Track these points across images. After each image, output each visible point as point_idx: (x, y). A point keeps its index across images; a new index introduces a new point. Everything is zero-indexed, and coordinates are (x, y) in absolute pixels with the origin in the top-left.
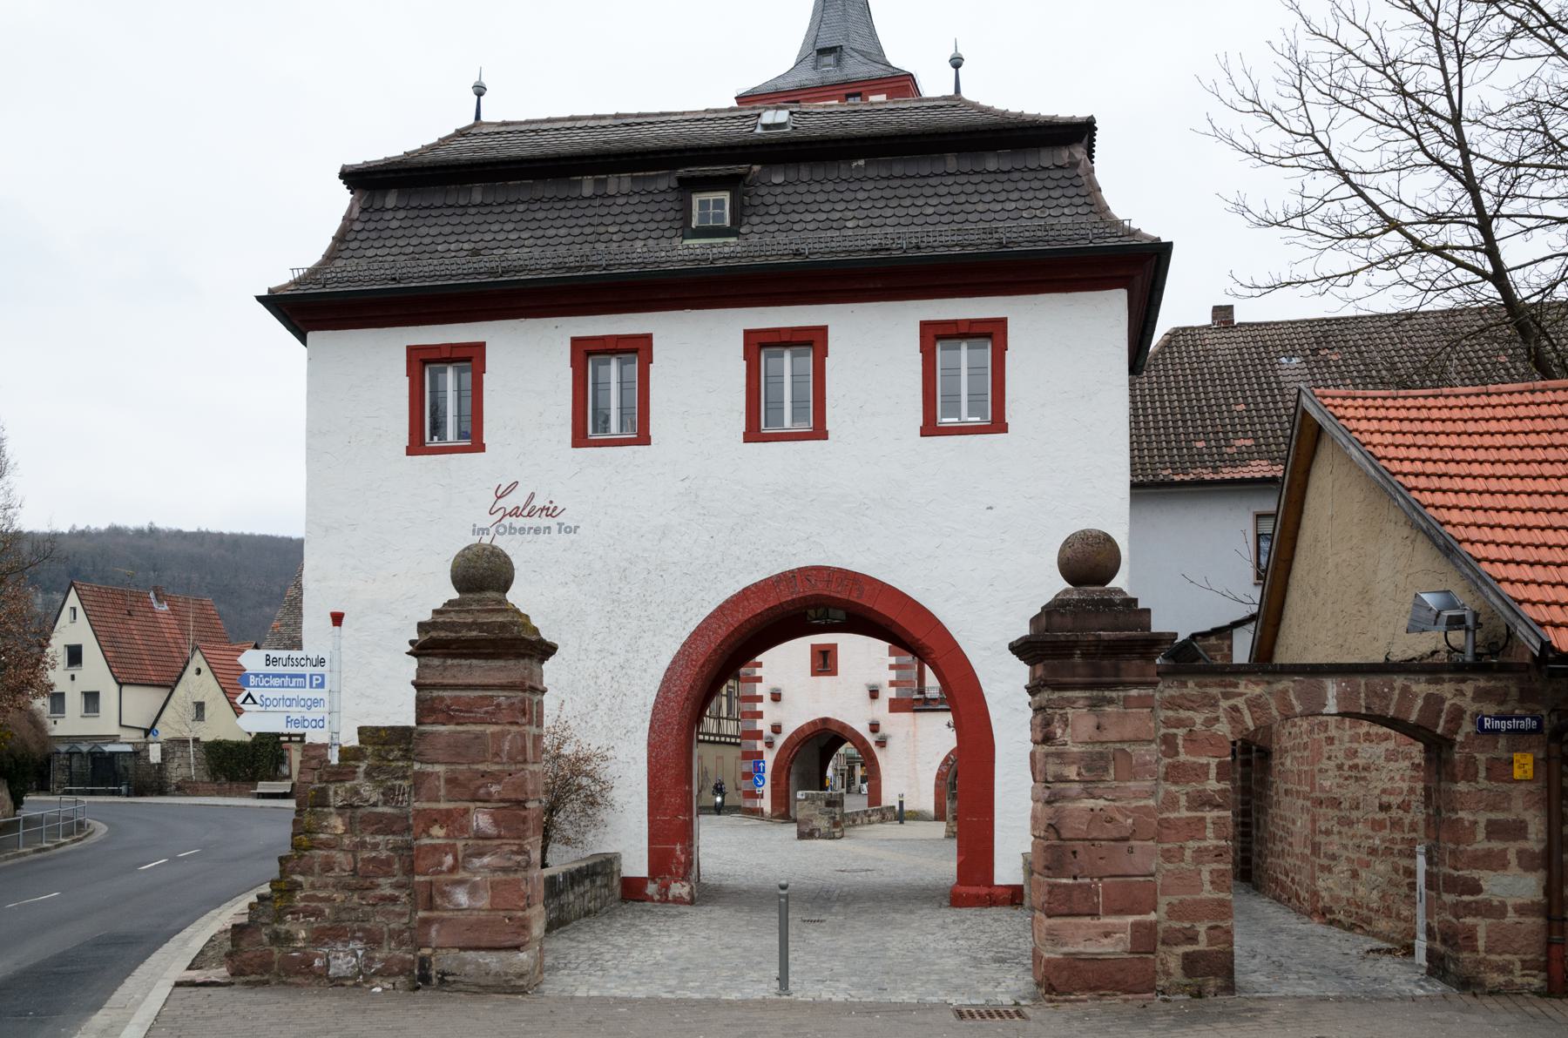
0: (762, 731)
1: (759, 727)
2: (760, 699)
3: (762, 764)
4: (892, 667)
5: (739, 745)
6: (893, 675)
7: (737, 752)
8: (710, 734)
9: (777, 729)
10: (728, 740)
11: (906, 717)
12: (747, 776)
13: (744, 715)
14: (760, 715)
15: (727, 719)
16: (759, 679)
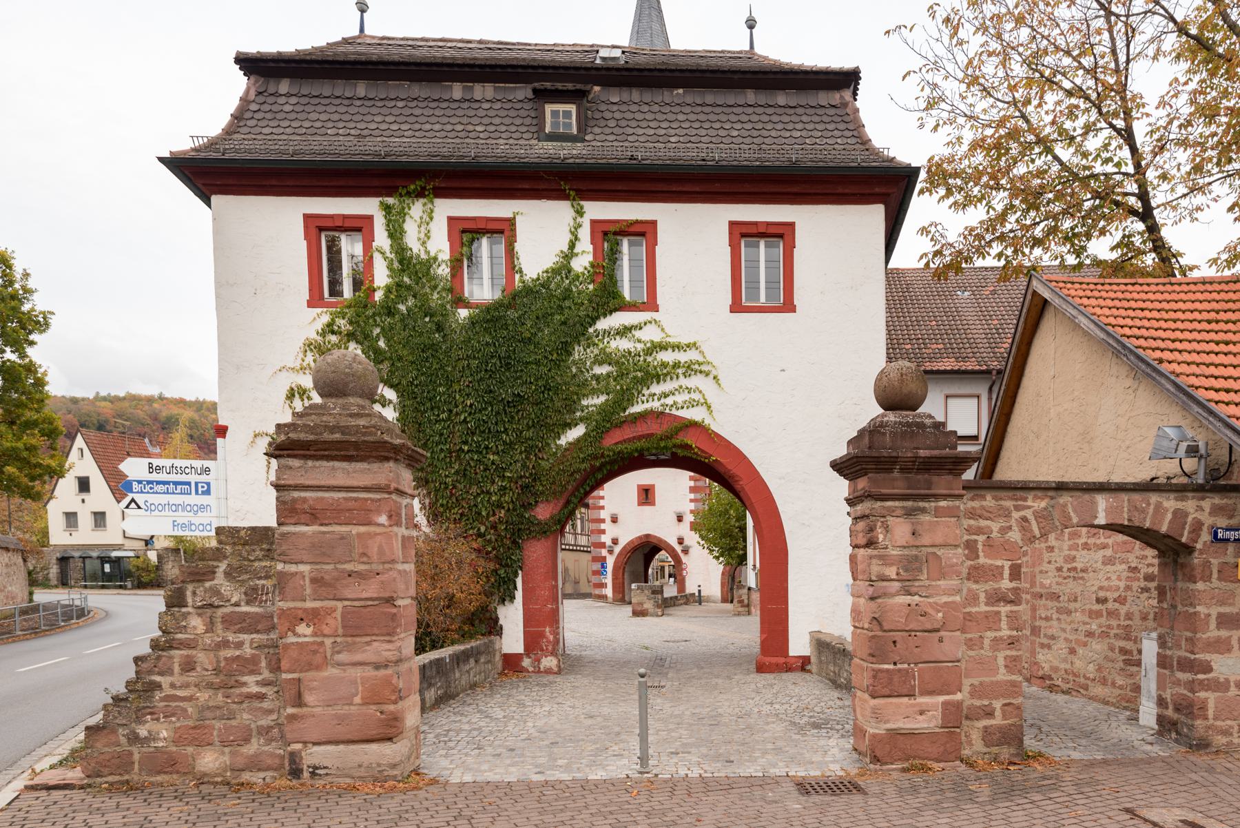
1: (603, 540)
2: (603, 521)
4: (691, 501)
6: (692, 506)
7: (588, 557)
8: (569, 545)
9: (615, 541)
12: (596, 573)
14: (603, 532)
16: (602, 508)
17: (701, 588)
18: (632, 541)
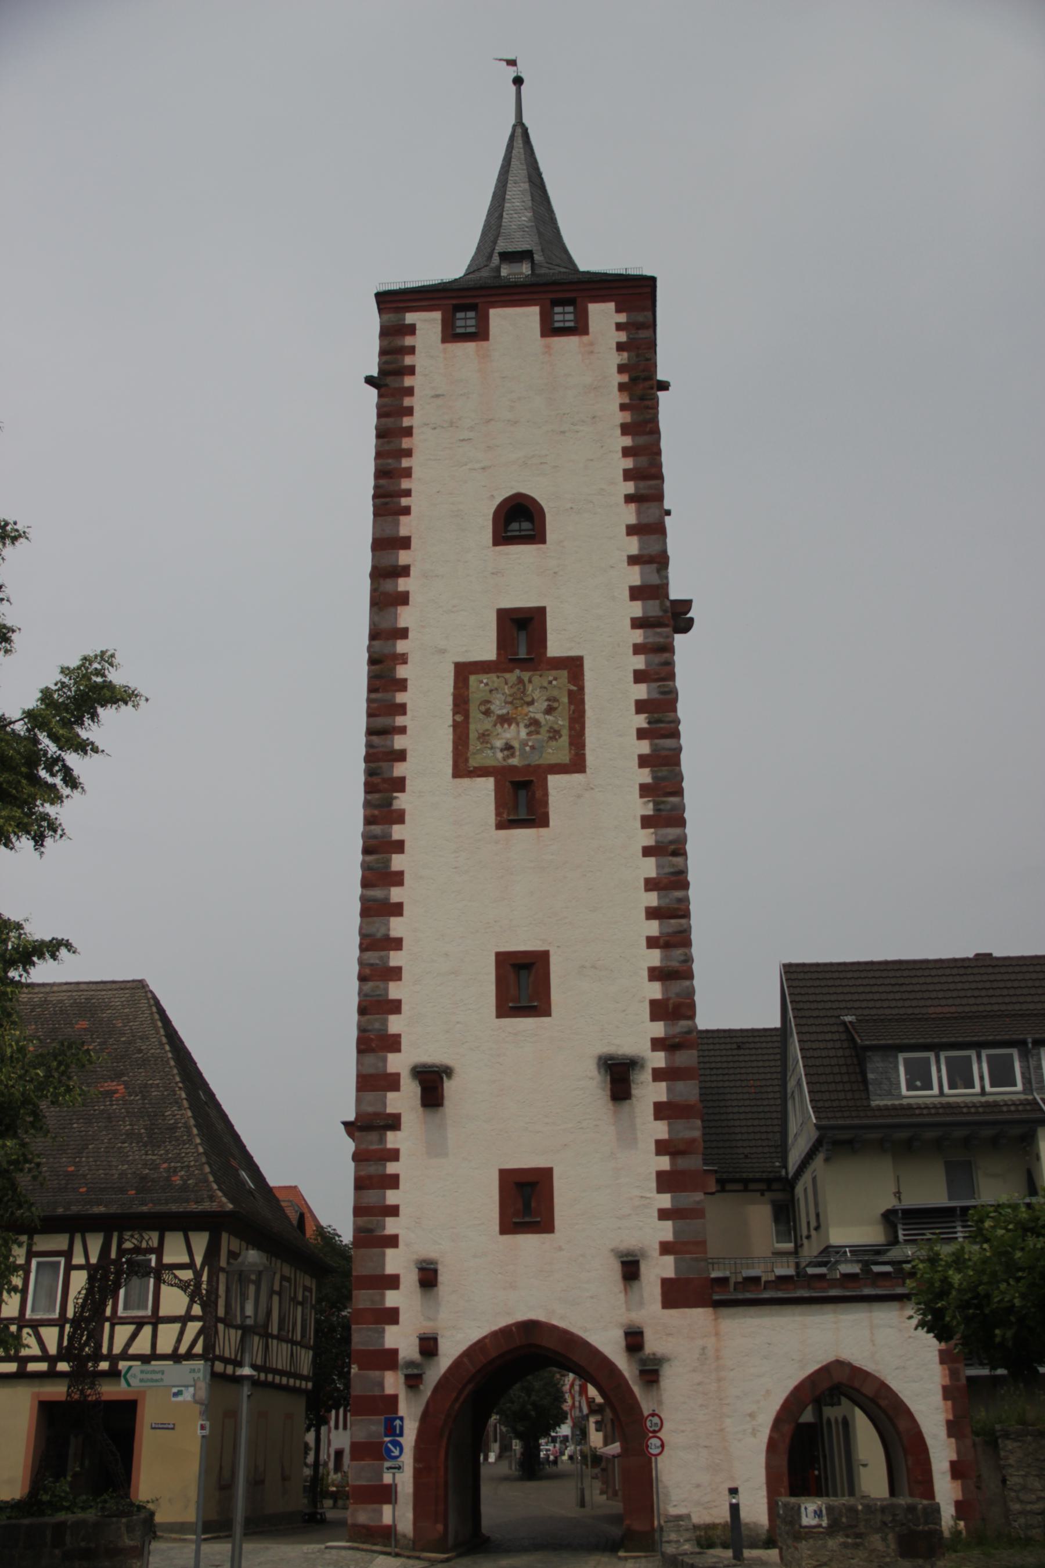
0: (395, 1352)
1: (390, 1342)
2: (393, 1282)
4: (664, 1214)
6: (666, 1231)
9: (429, 1346)
11: (700, 1316)
14: (392, 1316)
16: (393, 1241)
18: (477, 1348)
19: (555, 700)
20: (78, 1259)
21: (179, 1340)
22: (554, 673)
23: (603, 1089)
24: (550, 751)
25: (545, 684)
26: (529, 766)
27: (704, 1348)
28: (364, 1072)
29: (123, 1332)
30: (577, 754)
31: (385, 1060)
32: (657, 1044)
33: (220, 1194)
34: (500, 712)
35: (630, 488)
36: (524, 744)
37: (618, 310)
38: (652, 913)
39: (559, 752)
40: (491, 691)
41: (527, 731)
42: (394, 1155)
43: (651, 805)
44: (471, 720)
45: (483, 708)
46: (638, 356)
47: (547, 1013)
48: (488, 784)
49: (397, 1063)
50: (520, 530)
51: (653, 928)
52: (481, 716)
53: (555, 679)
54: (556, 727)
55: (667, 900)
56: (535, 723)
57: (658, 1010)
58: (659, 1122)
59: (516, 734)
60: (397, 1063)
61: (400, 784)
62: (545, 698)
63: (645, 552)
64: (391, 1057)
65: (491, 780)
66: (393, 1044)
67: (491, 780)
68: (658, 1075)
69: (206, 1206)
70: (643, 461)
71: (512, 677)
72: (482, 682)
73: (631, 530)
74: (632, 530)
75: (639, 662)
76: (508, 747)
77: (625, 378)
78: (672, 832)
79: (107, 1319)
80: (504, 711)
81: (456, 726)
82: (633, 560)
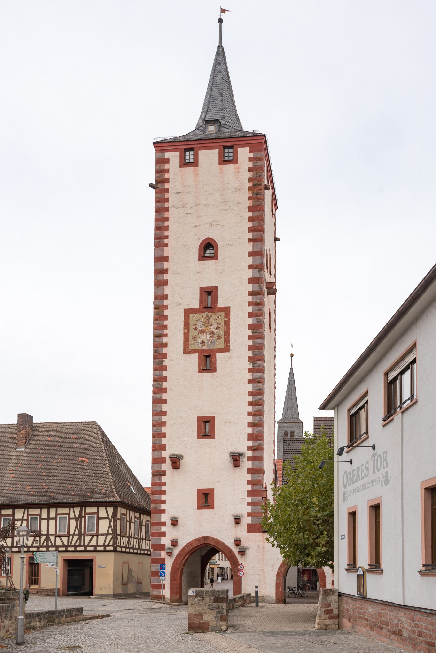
0: (164, 545)
2: (164, 524)
3: (164, 566)
4: (249, 504)
5: (150, 555)
6: (249, 509)
7: (148, 560)
8: (134, 549)
9: (174, 543)
10: (146, 552)
12: (155, 574)
13: (153, 534)
15: (145, 539)
16: (164, 511)
17: (259, 589)
18: (190, 543)
19: (220, 324)
20: (72, 516)
21: (105, 541)
22: (220, 313)
23: (231, 463)
24: (217, 344)
25: (216, 318)
26: (210, 349)
27: (259, 545)
28: (154, 457)
29: (88, 539)
30: (227, 345)
31: (161, 453)
32: (249, 449)
33: (116, 495)
34: (200, 329)
35: (250, 235)
36: (208, 341)
37: (250, 152)
38: (250, 404)
39: (220, 344)
40: (197, 320)
41: (210, 336)
42: (164, 484)
43: (251, 364)
44: (190, 332)
45: (194, 327)
46: (256, 174)
47: (214, 438)
48: (196, 356)
49: (165, 454)
50: (210, 254)
51: (250, 409)
52: (194, 330)
53: (220, 316)
54: (220, 335)
55: (255, 399)
56: (212, 333)
57: (250, 437)
58: (249, 474)
59: (205, 337)
60: (165, 454)
61: (165, 356)
62: (216, 323)
63: (255, 264)
64: (163, 452)
65: (197, 354)
66: (164, 448)
67: (197, 354)
68: (249, 459)
69: (112, 499)
70: (256, 223)
71: (205, 315)
72: (194, 317)
73: (250, 254)
74: (250, 254)
75: (250, 309)
76: (203, 342)
77: (251, 185)
78: (258, 375)
79: (82, 535)
80: (202, 328)
81: (185, 334)
82: (250, 267)
